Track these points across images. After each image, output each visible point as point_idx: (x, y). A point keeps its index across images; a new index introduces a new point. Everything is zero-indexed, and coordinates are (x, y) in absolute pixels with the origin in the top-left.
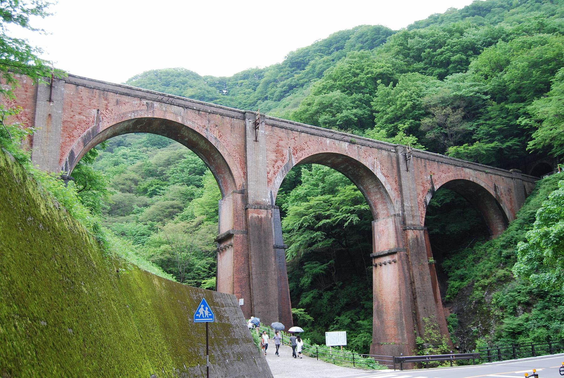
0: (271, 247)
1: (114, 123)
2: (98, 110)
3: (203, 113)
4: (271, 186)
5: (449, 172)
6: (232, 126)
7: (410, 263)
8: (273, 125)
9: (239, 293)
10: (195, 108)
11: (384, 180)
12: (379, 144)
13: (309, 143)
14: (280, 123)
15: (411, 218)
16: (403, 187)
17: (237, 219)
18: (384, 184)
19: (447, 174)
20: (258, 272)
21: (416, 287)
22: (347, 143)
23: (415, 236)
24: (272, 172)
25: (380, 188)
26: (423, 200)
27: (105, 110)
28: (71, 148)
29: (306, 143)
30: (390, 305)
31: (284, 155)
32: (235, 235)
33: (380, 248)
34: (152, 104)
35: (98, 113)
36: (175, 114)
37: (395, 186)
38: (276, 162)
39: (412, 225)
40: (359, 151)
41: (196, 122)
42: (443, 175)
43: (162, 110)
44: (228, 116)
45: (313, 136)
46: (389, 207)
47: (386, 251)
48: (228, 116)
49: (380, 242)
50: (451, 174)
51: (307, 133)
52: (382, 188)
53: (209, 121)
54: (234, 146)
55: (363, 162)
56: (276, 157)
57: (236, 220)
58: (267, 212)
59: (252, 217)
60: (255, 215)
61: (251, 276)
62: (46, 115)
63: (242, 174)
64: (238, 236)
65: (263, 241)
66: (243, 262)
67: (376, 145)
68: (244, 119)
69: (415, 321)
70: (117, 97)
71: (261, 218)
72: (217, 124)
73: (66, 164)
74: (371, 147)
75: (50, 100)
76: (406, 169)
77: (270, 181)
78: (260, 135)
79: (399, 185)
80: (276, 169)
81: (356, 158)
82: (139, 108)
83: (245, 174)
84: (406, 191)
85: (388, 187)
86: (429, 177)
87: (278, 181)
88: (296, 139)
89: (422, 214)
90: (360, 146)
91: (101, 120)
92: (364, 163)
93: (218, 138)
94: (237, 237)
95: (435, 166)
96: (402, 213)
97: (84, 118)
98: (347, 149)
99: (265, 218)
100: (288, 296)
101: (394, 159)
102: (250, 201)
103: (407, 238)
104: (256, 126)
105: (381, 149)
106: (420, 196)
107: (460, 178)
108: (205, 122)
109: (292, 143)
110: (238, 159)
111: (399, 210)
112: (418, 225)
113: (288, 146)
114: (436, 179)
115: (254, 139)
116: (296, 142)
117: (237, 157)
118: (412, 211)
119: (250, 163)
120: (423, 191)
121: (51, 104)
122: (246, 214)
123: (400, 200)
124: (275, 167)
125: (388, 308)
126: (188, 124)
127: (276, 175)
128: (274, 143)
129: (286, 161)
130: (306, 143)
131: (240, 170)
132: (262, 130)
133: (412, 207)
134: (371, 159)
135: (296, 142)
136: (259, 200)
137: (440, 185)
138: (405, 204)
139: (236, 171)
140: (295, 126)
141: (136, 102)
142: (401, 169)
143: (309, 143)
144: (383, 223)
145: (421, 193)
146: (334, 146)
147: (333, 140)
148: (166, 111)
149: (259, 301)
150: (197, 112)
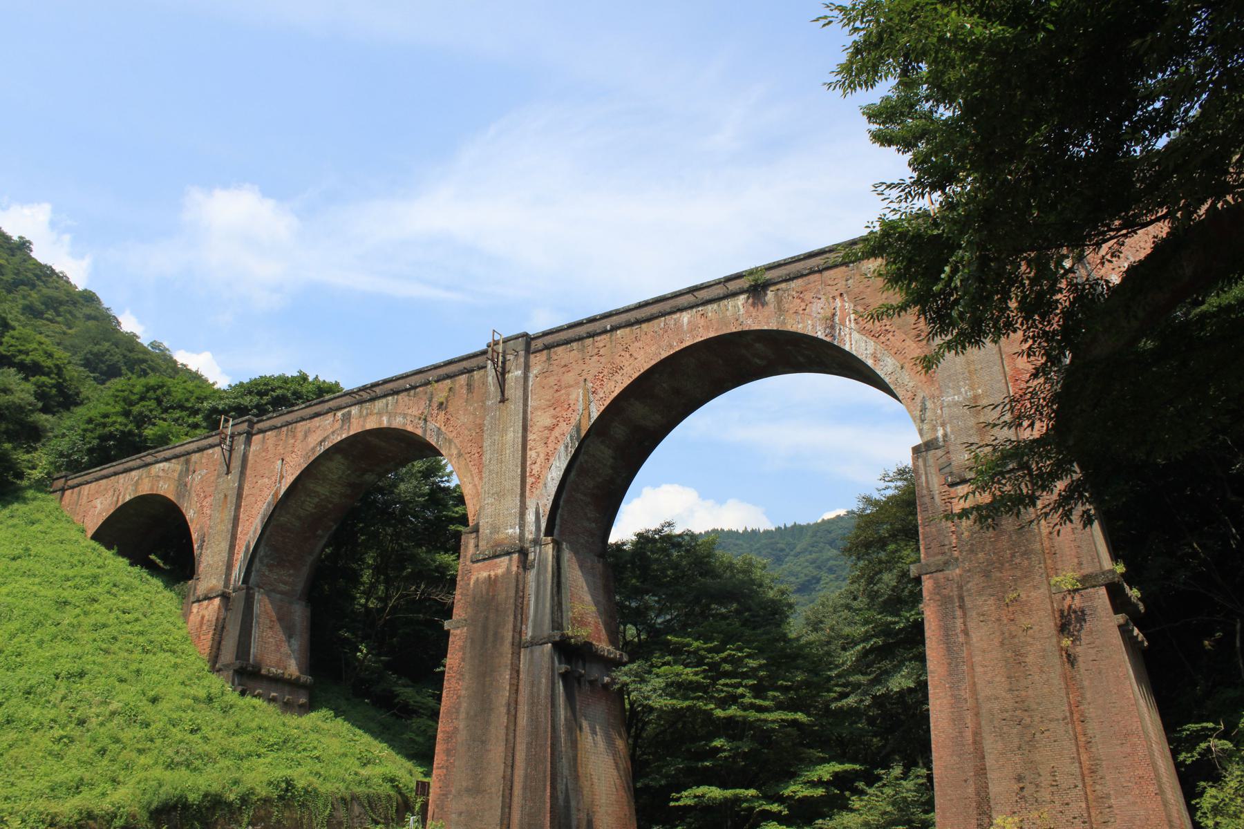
2: (283, 460)
11: (871, 350)
20: (472, 713)
28: (247, 538)
31: (572, 402)
32: (451, 631)
38: (551, 429)
41: (410, 411)
51: (629, 324)
54: (469, 430)
58: (510, 560)
60: (485, 574)
62: (222, 496)
65: (491, 633)
71: (496, 576)
75: (228, 473)
90: (783, 285)
98: (742, 311)
99: (503, 575)
100: (545, 772)
127: (552, 459)
128: (551, 387)
129: (575, 418)
134: (818, 308)
146: (702, 322)
148: (367, 414)
149: (465, 784)
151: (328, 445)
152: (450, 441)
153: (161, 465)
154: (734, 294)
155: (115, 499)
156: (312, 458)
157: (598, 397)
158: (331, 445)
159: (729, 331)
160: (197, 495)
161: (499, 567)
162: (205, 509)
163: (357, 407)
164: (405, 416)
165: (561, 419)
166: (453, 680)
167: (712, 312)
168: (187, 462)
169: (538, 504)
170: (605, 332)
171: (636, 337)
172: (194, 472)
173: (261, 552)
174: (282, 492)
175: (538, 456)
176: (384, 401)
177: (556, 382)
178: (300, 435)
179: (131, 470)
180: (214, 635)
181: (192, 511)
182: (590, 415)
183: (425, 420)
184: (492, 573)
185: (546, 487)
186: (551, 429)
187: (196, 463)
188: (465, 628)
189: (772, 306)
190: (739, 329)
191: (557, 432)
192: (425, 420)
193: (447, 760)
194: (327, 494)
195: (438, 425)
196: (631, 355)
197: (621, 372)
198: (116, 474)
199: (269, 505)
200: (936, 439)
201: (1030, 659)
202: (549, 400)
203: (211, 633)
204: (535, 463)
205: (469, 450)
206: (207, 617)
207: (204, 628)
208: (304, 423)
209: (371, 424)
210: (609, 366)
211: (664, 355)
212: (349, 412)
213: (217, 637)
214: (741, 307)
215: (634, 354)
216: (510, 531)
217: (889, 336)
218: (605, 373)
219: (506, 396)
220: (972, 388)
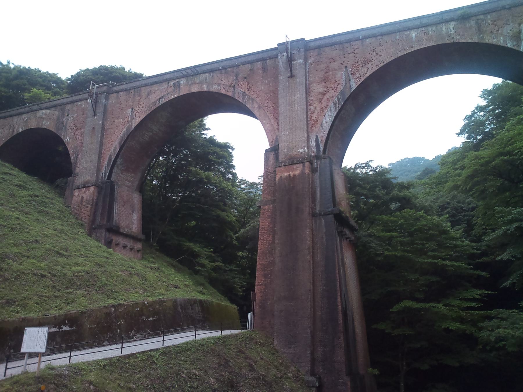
2: (132, 109)
3: (230, 69)
9: (262, 284)
28: (109, 153)
29: (374, 51)
32: (262, 207)
36: (201, 83)
38: (324, 94)
41: (223, 82)
54: (266, 94)
56: (325, 87)
58: (304, 166)
59: (281, 176)
60: (286, 174)
63: (276, 126)
64: (267, 207)
70: (148, 89)
71: (294, 175)
75: (95, 115)
82: (166, 92)
87: (328, 120)
90: (482, 17)
92: (494, 41)
94: (265, 209)
98: (453, 31)
99: (299, 175)
110: (272, 108)
113: (343, 66)
115: (289, 75)
116: (357, 56)
117: (269, 106)
121: (95, 118)
124: (323, 101)
126: (214, 88)
128: (322, 70)
129: (340, 88)
130: (374, 51)
135: (357, 56)
136: (294, 153)
141: (165, 86)
146: (425, 37)
148: (192, 84)
151: (164, 101)
152: (253, 100)
153: (44, 111)
155: (11, 130)
157: (355, 77)
159: (444, 42)
160: (71, 129)
161: (296, 170)
162: (77, 137)
163: (184, 79)
164: (219, 85)
165: (330, 89)
166: (265, 235)
167: (432, 31)
168: (63, 110)
169: (317, 136)
171: (380, 44)
172: (68, 115)
173: (119, 161)
174: (133, 127)
176: (204, 75)
177: (326, 68)
178: (144, 95)
179: (22, 114)
180: (91, 208)
181: (68, 138)
182: (350, 86)
183: (234, 87)
184: (291, 174)
185: (322, 127)
186: (324, 94)
187: (69, 110)
188: (272, 206)
189: (474, 29)
190: (452, 41)
191: (328, 96)
192: (234, 87)
193: (265, 281)
194: (157, 131)
195: (243, 91)
196: (377, 54)
198: (11, 116)
199: (124, 134)
202: (322, 78)
203: (89, 208)
204: (314, 113)
205: (266, 105)
206: (85, 198)
207: (84, 204)
208: (147, 87)
209: (195, 89)
210: (362, 59)
211: (400, 54)
212: (179, 82)
213: (93, 210)
214: (452, 29)
216: (301, 150)
219: (293, 74)
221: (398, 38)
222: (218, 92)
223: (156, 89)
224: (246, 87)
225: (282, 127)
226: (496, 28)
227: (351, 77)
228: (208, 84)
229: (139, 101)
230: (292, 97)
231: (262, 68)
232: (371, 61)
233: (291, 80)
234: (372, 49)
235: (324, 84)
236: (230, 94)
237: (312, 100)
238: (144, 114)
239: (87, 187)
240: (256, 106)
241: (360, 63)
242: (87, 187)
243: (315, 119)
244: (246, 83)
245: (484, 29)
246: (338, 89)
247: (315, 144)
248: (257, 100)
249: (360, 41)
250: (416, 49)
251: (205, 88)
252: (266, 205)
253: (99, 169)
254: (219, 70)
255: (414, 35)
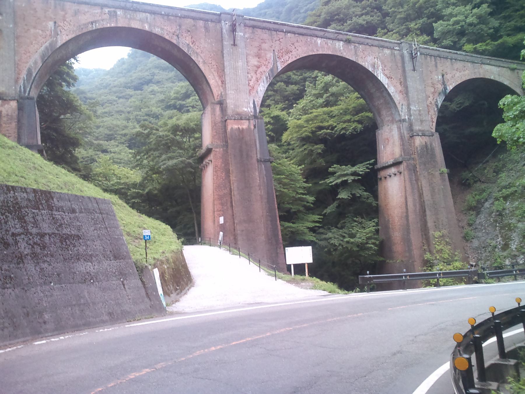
0: (254, 161)
1: (73, 36)
2: (55, 23)
3: (172, 18)
4: (254, 94)
5: (464, 71)
6: (207, 29)
7: (418, 173)
8: (254, 27)
9: (220, 211)
10: (163, 13)
11: (387, 82)
12: (381, 42)
13: (296, 44)
14: (262, 23)
15: (420, 123)
16: (409, 89)
17: (216, 132)
18: (386, 86)
19: (462, 73)
21: (425, 200)
22: (342, 42)
23: (424, 143)
24: (254, 79)
25: (383, 91)
26: (433, 102)
27: (62, 22)
28: (28, 66)
29: (293, 44)
30: (396, 219)
31: (268, 59)
32: (213, 149)
33: (385, 159)
34: (115, 12)
35: (55, 26)
37: (400, 88)
38: (258, 67)
39: (420, 130)
40: (356, 51)
41: (166, 28)
42: (458, 74)
43: (126, 17)
44: (201, 19)
45: (301, 37)
46: (393, 112)
47: (391, 162)
48: (201, 19)
49: (385, 152)
50: (467, 72)
51: (294, 33)
52: (385, 92)
53: (180, 26)
54: (209, 52)
55: (361, 62)
56: (258, 62)
57: (215, 133)
58: (249, 122)
59: (232, 128)
60: (236, 127)
61: (232, 193)
63: (220, 83)
64: (218, 150)
66: (224, 178)
67: (376, 43)
68: (220, 21)
69: (424, 236)
71: (243, 129)
72: (189, 29)
73: (24, 84)
74: (370, 46)
76: (412, 68)
77: (252, 89)
78: (238, 38)
79: (404, 86)
80: (259, 75)
81: (353, 59)
82: (100, 18)
83: (223, 82)
84: (412, 93)
85: (391, 90)
86: (440, 77)
87: (262, 89)
88: (281, 40)
89: (432, 118)
90: (357, 45)
91: (59, 33)
92: (363, 64)
93: (191, 44)
94: (216, 151)
95: (447, 63)
96: (408, 118)
97: (40, 32)
98: (342, 48)
99: (246, 129)
101: (398, 57)
102: (229, 112)
103: (414, 146)
104: (233, 29)
105: (383, 47)
106: (430, 99)
107: (478, 77)
108: (174, 28)
109: (277, 46)
110: (215, 66)
111: (405, 115)
112: (428, 131)
113: (272, 49)
114: (448, 78)
115: (232, 43)
116: (282, 44)
117: (213, 64)
118: (420, 115)
119: (228, 70)
120: (434, 93)
122: (225, 127)
123: (406, 104)
124: (258, 73)
125: (395, 223)
126: (157, 31)
128: (256, 47)
129: (270, 66)
130: (293, 44)
131: (217, 78)
132: (241, 32)
133: (420, 111)
137: (454, 85)
138: (412, 108)
139: (213, 80)
140: (280, 26)
141: (98, 11)
142: (407, 69)
143: (296, 44)
144: (387, 130)
145: (431, 96)
146: (326, 46)
147: (325, 40)
150: (166, 17)
151: (98, 26)
154: (339, 40)
156: (85, 31)
157: (280, 60)
158: (101, 27)
161: (244, 125)
164: (162, 29)
169: (254, 100)
170: (282, 31)
175: (252, 77)
176: (144, 14)
188: (222, 149)
190: (341, 55)
191: (261, 70)
192: (178, 36)
195: (187, 42)
197: (291, 54)
200: (406, 119)
201: (436, 190)
205: (210, 62)
210: (285, 48)
211: (311, 53)
215: (297, 48)
216: (246, 109)
217: (392, 79)
218: (284, 50)
220: (419, 107)
221: (309, 40)
222: (161, 35)
223: (86, 10)
224: (190, 40)
225: (229, 86)
226: (364, 57)
227: (278, 59)
228: (150, 26)
229: (64, 16)
230: (236, 63)
231: (205, 27)
232: (291, 51)
233: (234, 48)
234: (292, 43)
235: (257, 59)
236: (174, 42)
237: (249, 69)
238: (73, 33)
239: (5, 100)
240: (201, 60)
241: (284, 50)
242: (5, 100)
243: (252, 86)
244: (190, 36)
245: (358, 54)
246: (268, 67)
247: (252, 106)
248: (202, 55)
249: (284, 33)
250: (321, 53)
251: (147, 28)
252: (218, 148)
253: (17, 81)
254: (161, 14)
255: (319, 42)
